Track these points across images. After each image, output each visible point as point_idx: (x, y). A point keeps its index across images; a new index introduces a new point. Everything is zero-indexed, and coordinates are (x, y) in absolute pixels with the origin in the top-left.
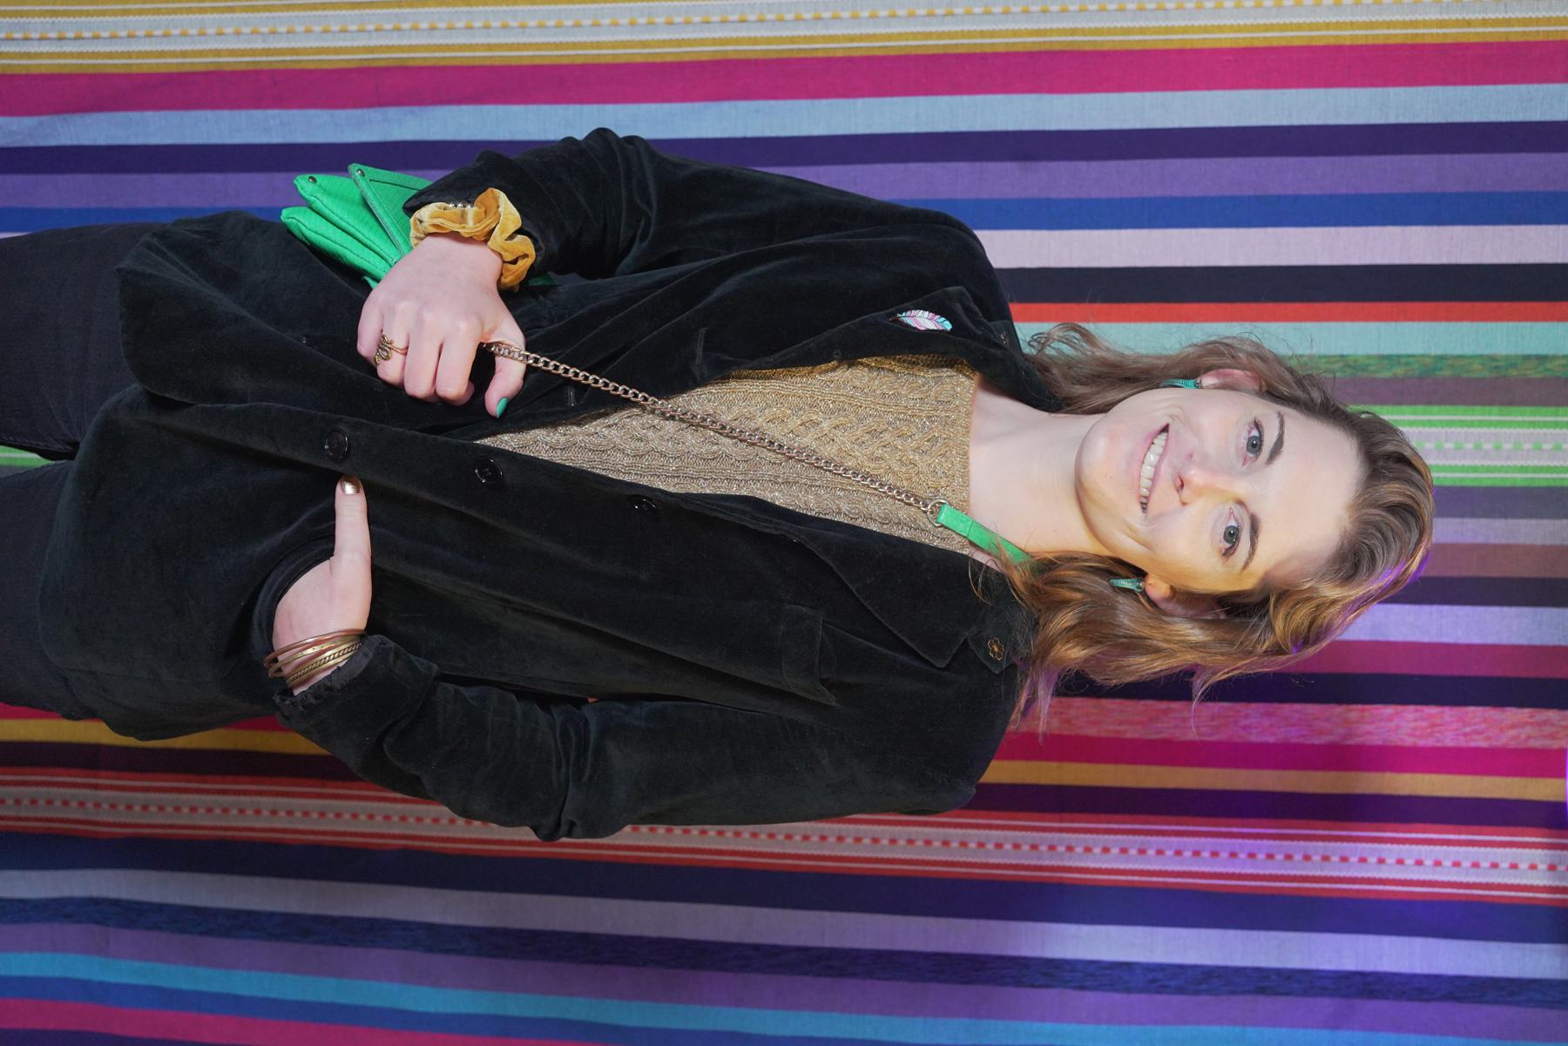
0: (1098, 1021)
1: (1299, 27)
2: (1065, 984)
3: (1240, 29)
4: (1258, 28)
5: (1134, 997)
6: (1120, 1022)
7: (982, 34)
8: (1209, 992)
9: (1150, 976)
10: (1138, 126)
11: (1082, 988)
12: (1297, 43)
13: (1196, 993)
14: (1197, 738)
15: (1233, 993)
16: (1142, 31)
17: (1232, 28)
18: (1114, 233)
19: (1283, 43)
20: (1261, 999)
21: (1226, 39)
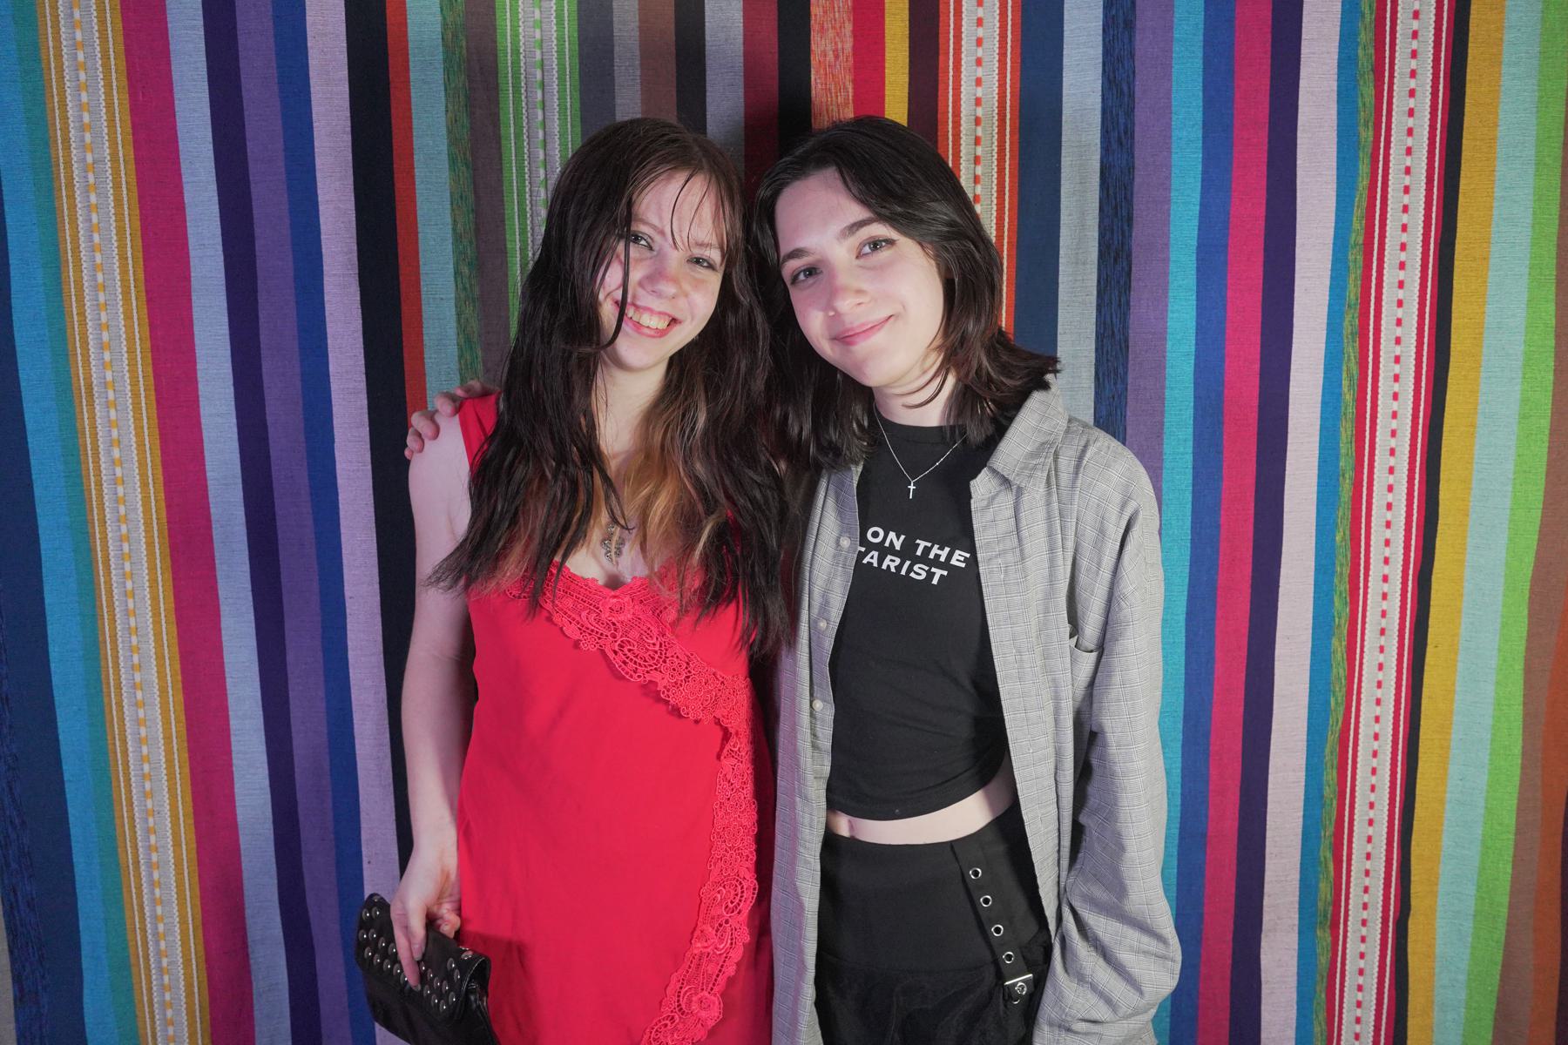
0: (1167, 201)
1: (102, 22)
2: (1126, 236)
3: (108, 85)
4: (106, 66)
5: (1137, 163)
6: (1169, 178)
7: (131, 351)
8: (1131, 86)
9: (1115, 146)
10: (214, 187)
11: (1130, 219)
12: (120, 26)
13: (1132, 96)
14: (851, 105)
15: (1132, 56)
16: (117, 186)
17: (108, 94)
18: (321, 208)
19: (121, 39)
20: (1139, 24)
21: (120, 99)
